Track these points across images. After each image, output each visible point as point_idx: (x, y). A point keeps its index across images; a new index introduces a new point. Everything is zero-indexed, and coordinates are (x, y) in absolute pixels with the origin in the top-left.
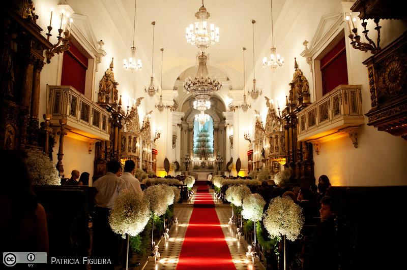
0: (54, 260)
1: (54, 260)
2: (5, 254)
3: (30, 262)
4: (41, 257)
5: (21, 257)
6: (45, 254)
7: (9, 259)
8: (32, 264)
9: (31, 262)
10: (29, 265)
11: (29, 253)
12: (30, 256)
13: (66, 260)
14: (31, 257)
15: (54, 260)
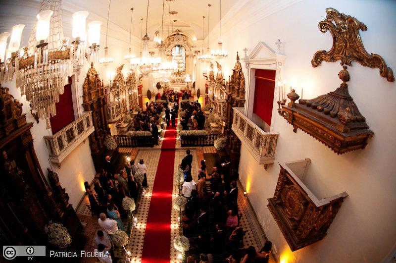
3: (29, 255)
6: (44, 247)
7: (9, 253)
8: (31, 257)
9: (31, 255)
10: (28, 258)
14: (30, 251)
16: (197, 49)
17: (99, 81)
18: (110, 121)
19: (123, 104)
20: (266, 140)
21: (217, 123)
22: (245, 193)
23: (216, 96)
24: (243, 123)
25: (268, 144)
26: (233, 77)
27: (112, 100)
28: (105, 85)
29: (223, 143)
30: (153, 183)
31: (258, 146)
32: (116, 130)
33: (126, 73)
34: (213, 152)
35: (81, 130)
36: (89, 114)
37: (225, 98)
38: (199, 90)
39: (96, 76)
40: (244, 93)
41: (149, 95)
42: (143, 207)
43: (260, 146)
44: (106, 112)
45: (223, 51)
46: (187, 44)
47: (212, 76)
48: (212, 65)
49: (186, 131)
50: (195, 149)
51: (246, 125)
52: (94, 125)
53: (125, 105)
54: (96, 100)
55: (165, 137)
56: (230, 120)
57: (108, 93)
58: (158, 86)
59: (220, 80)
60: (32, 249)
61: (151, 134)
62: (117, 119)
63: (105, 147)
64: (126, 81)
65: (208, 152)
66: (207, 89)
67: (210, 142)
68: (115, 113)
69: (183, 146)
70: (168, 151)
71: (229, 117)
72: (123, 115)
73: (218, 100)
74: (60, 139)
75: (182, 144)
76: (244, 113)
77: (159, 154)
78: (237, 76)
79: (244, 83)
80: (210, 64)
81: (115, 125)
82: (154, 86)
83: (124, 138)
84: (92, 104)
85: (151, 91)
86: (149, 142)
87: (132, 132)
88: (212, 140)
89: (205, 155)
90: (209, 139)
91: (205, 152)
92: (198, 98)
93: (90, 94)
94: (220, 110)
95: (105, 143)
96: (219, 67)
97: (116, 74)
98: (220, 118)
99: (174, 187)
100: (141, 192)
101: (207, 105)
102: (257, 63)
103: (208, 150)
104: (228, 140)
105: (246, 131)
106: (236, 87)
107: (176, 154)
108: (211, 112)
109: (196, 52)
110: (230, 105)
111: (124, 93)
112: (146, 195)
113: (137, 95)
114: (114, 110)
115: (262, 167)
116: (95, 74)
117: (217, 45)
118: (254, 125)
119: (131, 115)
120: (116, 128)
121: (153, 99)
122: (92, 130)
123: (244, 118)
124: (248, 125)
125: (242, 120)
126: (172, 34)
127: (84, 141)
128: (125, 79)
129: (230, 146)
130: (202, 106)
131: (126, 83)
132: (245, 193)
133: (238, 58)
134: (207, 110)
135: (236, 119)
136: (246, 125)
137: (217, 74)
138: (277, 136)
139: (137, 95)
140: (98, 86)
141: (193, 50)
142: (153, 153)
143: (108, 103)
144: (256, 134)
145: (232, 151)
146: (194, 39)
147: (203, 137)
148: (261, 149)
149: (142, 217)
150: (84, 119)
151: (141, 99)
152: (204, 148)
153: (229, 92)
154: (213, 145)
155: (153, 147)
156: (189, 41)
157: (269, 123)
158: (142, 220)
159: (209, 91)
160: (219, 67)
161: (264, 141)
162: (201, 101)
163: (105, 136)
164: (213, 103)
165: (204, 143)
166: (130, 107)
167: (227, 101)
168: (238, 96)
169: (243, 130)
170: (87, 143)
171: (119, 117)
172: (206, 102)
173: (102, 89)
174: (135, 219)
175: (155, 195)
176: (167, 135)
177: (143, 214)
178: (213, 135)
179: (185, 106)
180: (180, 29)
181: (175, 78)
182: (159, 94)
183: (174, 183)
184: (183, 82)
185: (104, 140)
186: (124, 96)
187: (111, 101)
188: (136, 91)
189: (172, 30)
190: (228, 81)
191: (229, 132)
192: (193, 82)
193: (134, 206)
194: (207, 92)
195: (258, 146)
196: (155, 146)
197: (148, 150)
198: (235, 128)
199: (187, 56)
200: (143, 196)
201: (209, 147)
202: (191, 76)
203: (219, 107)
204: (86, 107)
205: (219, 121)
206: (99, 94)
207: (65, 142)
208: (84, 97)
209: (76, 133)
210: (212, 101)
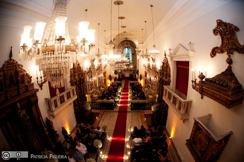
0: (32, 156)
1: (32, 156)
2: (3, 152)
3: (18, 157)
4: (24, 154)
5: (13, 154)
6: (27, 152)
8: (19, 158)
9: (19, 157)
10: (17, 159)
11: (17, 152)
12: (18, 153)
13: (39, 156)
15: (32, 156)
17: (80, 68)
20: (185, 104)
21: (153, 96)
22: (170, 138)
23: (152, 79)
24: (170, 94)
26: (162, 66)
28: (84, 70)
29: (157, 107)
30: (113, 132)
31: (180, 109)
32: (90, 99)
33: (96, 64)
34: (150, 113)
35: (69, 97)
36: (74, 88)
37: (158, 80)
38: (141, 75)
39: (79, 64)
40: (170, 76)
41: (110, 78)
42: (106, 146)
43: (181, 108)
44: (84, 88)
47: (149, 66)
48: (149, 60)
50: (140, 112)
51: (172, 96)
52: (77, 94)
53: (96, 83)
54: (78, 79)
55: (120, 104)
56: (161, 94)
57: (85, 75)
58: (116, 72)
59: (154, 68)
60: (20, 153)
62: (91, 92)
63: (83, 108)
64: (96, 69)
65: (147, 114)
66: (146, 74)
67: (149, 107)
69: (132, 109)
70: (123, 112)
71: (161, 91)
72: (95, 90)
73: (153, 81)
75: (131, 108)
76: (171, 88)
77: (117, 114)
78: (165, 66)
79: (170, 70)
80: (147, 59)
81: (90, 95)
82: (113, 72)
83: (95, 103)
84: (76, 82)
85: (112, 75)
86: (111, 107)
88: (150, 106)
89: (146, 116)
90: (148, 106)
91: (145, 113)
92: (141, 80)
93: (75, 76)
94: (155, 87)
95: (83, 106)
96: (154, 60)
97: (91, 64)
98: (155, 92)
99: (126, 134)
100: (106, 137)
101: (146, 85)
102: (176, 57)
103: (147, 112)
104: (160, 106)
105: (172, 100)
106: (165, 73)
108: (149, 89)
111: (95, 76)
112: (108, 139)
113: (103, 78)
114: (90, 86)
115: (182, 121)
116: (78, 63)
117: (153, 47)
118: (177, 96)
119: (100, 90)
120: (90, 98)
121: (113, 81)
122: (76, 97)
123: (171, 92)
124: (173, 96)
125: (170, 94)
127: (70, 104)
128: (96, 68)
129: (161, 109)
130: (142, 85)
131: (97, 70)
132: (170, 138)
133: (165, 55)
134: (146, 88)
135: (166, 93)
136: (172, 96)
137: (153, 65)
138: (191, 102)
139: (103, 78)
140: (80, 71)
142: (113, 114)
143: (86, 81)
144: (178, 101)
145: (163, 112)
148: (182, 110)
149: (106, 151)
150: (71, 91)
151: (105, 80)
152: (145, 111)
153: (161, 76)
154: (151, 109)
155: (113, 110)
157: (186, 94)
158: (105, 153)
159: (147, 76)
161: (183, 106)
162: (142, 82)
163: (83, 103)
164: (150, 83)
165: (145, 108)
166: (99, 85)
167: (159, 81)
168: (166, 79)
170: (72, 105)
171: (93, 91)
173: (82, 73)
174: (101, 153)
175: (114, 139)
176: (122, 102)
177: (106, 150)
178: (151, 103)
179: (132, 85)
182: (116, 77)
183: (126, 132)
185: (83, 104)
186: (95, 78)
187: (87, 81)
188: (102, 75)
190: (160, 69)
191: (160, 100)
193: (101, 145)
194: (146, 76)
195: (180, 109)
196: (114, 109)
197: (109, 111)
198: (165, 98)
200: (107, 139)
201: (148, 110)
203: (154, 86)
204: (72, 83)
206: (80, 76)
208: (71, 77)
209: (66, 99)
210: (150, 82)
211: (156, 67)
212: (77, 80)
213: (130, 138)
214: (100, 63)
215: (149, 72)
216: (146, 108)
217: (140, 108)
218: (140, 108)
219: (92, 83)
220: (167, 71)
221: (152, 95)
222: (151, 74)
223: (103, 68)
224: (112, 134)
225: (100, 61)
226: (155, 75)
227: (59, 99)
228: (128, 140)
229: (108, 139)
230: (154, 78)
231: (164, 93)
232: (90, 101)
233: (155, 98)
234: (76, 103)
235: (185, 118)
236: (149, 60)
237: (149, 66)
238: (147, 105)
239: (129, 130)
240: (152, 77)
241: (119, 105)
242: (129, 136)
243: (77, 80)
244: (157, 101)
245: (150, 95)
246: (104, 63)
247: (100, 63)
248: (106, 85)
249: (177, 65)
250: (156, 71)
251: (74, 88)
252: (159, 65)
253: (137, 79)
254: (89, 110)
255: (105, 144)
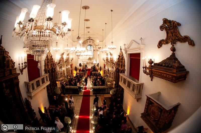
16: (99, 47)
17: (52, 59)
18: (57, 80)
19: (64, 72)
21: (111, 83)
23: (110, 69)
24: (125, 80)
25: (138, 89)
26: (118, 59)
27: (58, 70)
29: (114, 91)
30: (79, 111)
31: (133, 90)
32: (60, 85)
33: (65, 57)
35: (43, 82)
36: (48, 75)
37: (114, 70)
38: (101, 67)
39: (51, 56)
41: (76, 69)
42: (74, 122)
43: (135, 89)
45: (114, 46)
46: (94, 44)
47: (107, 59)
48: (107, 54)
49: (96, 87)
50: (100, 95)
51: (127, 81)
52: (49, 81)
54: (51, 68)
55: (84, 90)
56: (118, 81)
58: (80, 65)
59: (112, 60)
61: (78, 88)
62: (61, 79)
63: (55, 92)
64: (65, 61)
65: (106, 97)
66: (105, 66)
67: (107, 92)
68: (60, 76)
69: (94, 94)
71: (117, 78)
72: (63, 78)
74: (33, 84)
75: (93, 93)
76: (125, 75)
77: (82, 98)
78: (121, 58)
79: (124, 61)
80: (106, 53)
81: (59, 82)
82: (78, 65)
84: (49, 70)
85: (77, 67)
86: (76, 92)
87: (68, 87)
88: (108, 91)
91: (105, 97)
92: (100, 71)
93: (48, 65)
95: (55, 90)
96: (111, 54)
98: (113, 80)
99: (90, 113)
100: (74, 115)
101: (105, 74)
102: (131, 51)
104: (117, 90)
105: (126, 84)
106: (121, 64)
107: (90, 97)
108: (107, 77)
109: (99, 48)
110: (117, 73)
112: (76, 117)
113: (70, 69)
116: (51, 55)
118: (131, 80)
119: (67, 78)
120: (60, 84)
121: (78, 71)
122: (49, 83)
123: (125, 78)
124: (128, 81)
125: (124, 79)
126: (87, 39)
127: (44, 88)
129: (118, 93)
131: (65, 62)
133: (121, 50)
135: (121, 79)
136: (127, 81)
137: (110, 58)
139: (70, 69)
140: (52, 61)
141: (97, 47)
142: (79, 97)
145: (119, 95)
146: (97, 42)
147: (104, 89)
148: (135, 91)
149: (74, 127)
150: (45, 77)
152: (105, 95)
154: (110, 93)
155: (79, 94)
156: (95, 43)
157: (138, 80)
158: (74, 128)
159: (106, 67)
160: (111, 54)
162: (102, 73)
163: (55, 87)
164: (108, 73)
165: (104, 92)
167: (116, 71)
168: (122, 68)
169: (125, 84)
170: (46, 89)
172: (104, 73)
174: (71, 128)
175: (81, 117)
177: (75, 126)
178: (109, 88)
180: (91, 36)
181: (88, 61)
182: (80, 69)
183: (90, 111)
184: (92, 63)
185: (54, 89)
186: (64, 69)
187: (58, 70)
188: (70, 67)
189: (86, 37)
190: (116, 61)
191: (117, 85)
192: (97, 63)
193: (71, 121)
194: (105, 68)
195: (133, 90)
197: (76, 95)
198: (121, 84)
199: (94, 50)
200: (75, 117)
201: (107, 95)
202: (96, 61)
204: (46, 71)
205: (112, 81)
206: (52, 66)
207: (35, 87)
208: (45, 66)
209: (41, 83)
210: (108, 72)
211: (113, 59)
212: (50, 69)
213: (94, 116)
214: (68, 57)
215: (107, 65)
216: (105, 93)
217: (100, 93)
218: (100, 93)
219: (61, 72)
220: (122, 62)
221: (111, 81)
222: (109, 66)
223: (70, 61)
224: (78, 113)
225: (68, 55)
226: (112, 66)
227: (36, 83)
228: (92, 117)
229: (76, 117)
230: (111, 68)
231: (120, 79)
232: (60, 87)
233: (113, 84)
234: (49, 88)
235: (138, 98)
236: (107, 54)
237: (107, 59)
238: (106, 90)
239: (92, 110)
240: (110, 68)
241: (83, 91)
242: (93, 115)
243: (50, 69)
244: (114, 87)
245: (108, 82)
246: (71, 57)
247: (68, 57)
248: (72, 75)
249: (130, 57)
250: (113, 63)
251: (48, 75)
252: (115, 58)
253: (98, 71)
254: (59, 93)
255: (73, 121)
